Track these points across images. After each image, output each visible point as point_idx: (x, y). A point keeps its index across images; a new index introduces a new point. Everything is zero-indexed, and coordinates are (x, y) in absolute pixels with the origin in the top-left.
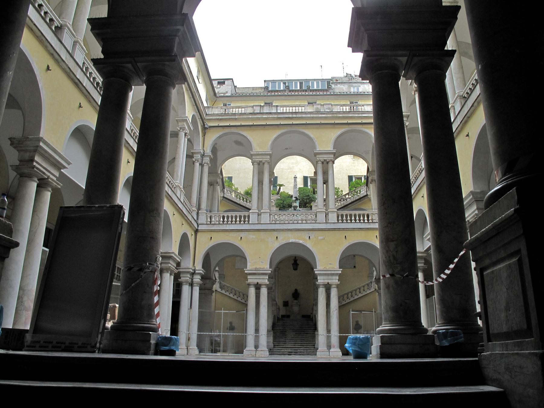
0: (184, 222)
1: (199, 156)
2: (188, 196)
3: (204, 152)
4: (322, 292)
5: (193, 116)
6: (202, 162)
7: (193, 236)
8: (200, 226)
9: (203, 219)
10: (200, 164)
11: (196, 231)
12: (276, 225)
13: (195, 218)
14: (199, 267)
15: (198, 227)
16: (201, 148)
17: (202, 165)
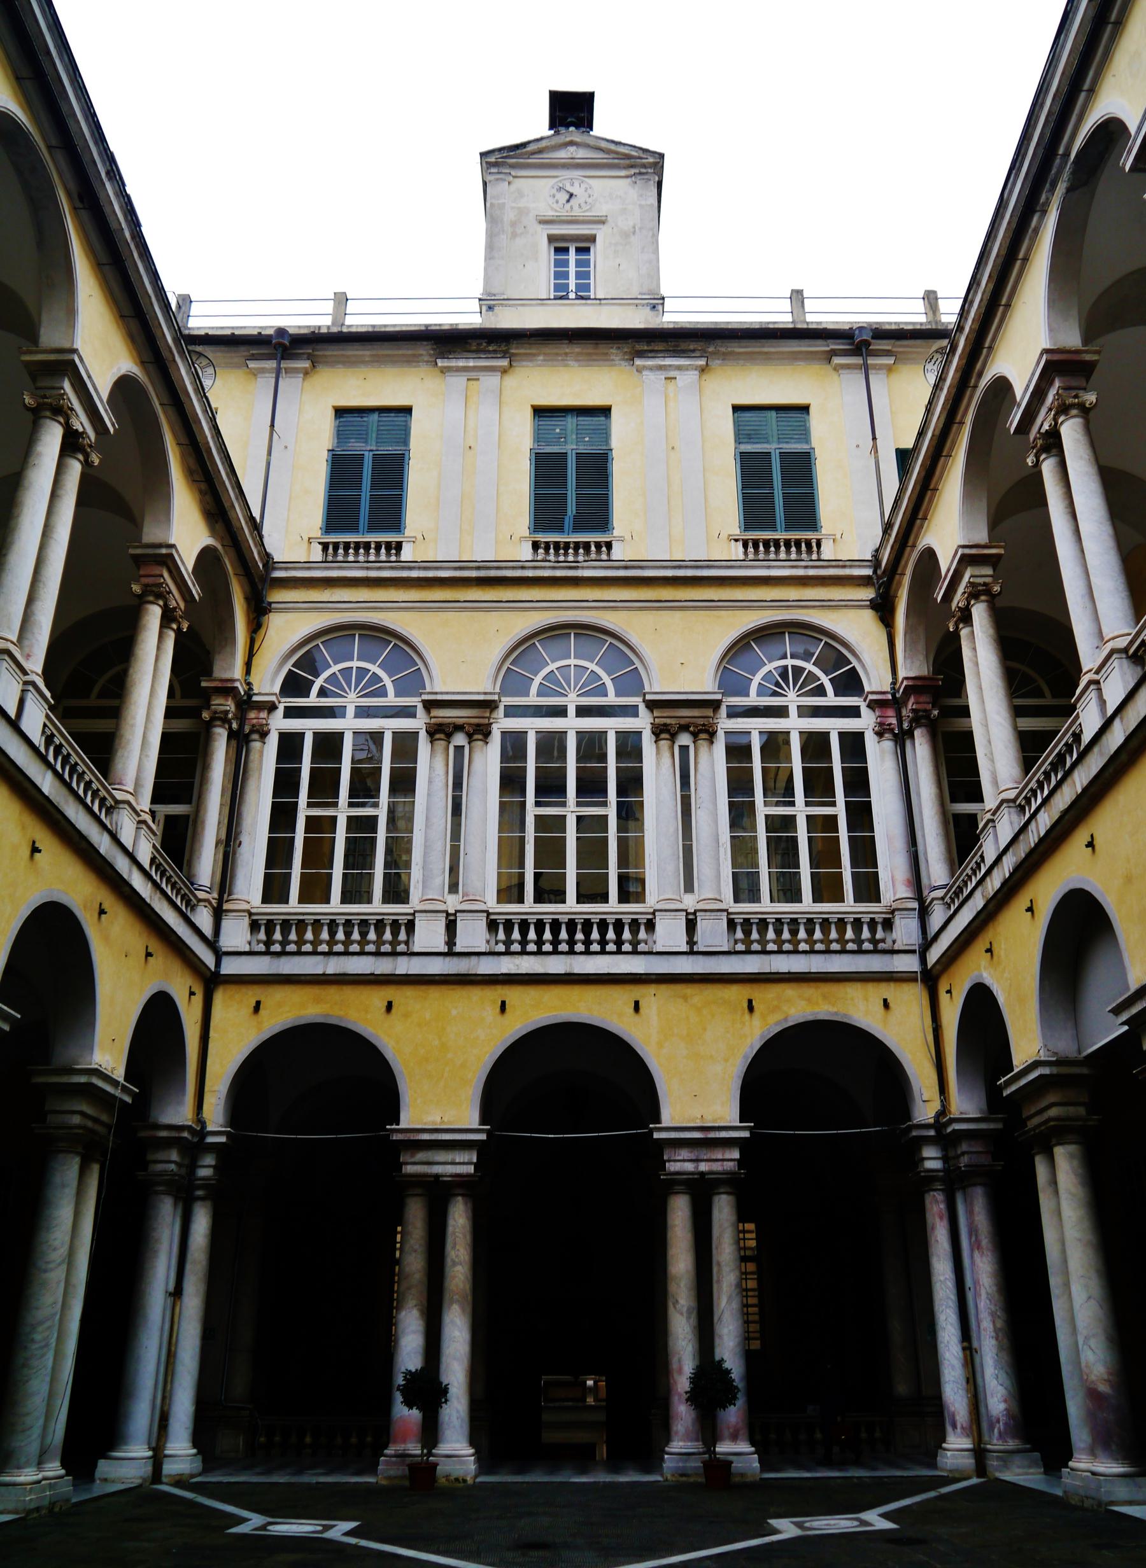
0: (155, 946)
1: (230, 705)
2: (177, 841)
3: (249, 693)
4: (680, 1211)
5: (206, 556)
6: (241, 726)
7: (198, 1000)
8: (226, 961)
9: (235, 934)
10: (231, 735)
11: (211, 982)
12: (814, 957)
13: (207, 930)
14: (215, 1114)
15: (218, 964)
16: (238, 672)
17: (241, 741)
